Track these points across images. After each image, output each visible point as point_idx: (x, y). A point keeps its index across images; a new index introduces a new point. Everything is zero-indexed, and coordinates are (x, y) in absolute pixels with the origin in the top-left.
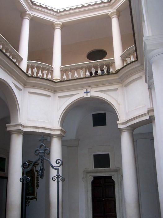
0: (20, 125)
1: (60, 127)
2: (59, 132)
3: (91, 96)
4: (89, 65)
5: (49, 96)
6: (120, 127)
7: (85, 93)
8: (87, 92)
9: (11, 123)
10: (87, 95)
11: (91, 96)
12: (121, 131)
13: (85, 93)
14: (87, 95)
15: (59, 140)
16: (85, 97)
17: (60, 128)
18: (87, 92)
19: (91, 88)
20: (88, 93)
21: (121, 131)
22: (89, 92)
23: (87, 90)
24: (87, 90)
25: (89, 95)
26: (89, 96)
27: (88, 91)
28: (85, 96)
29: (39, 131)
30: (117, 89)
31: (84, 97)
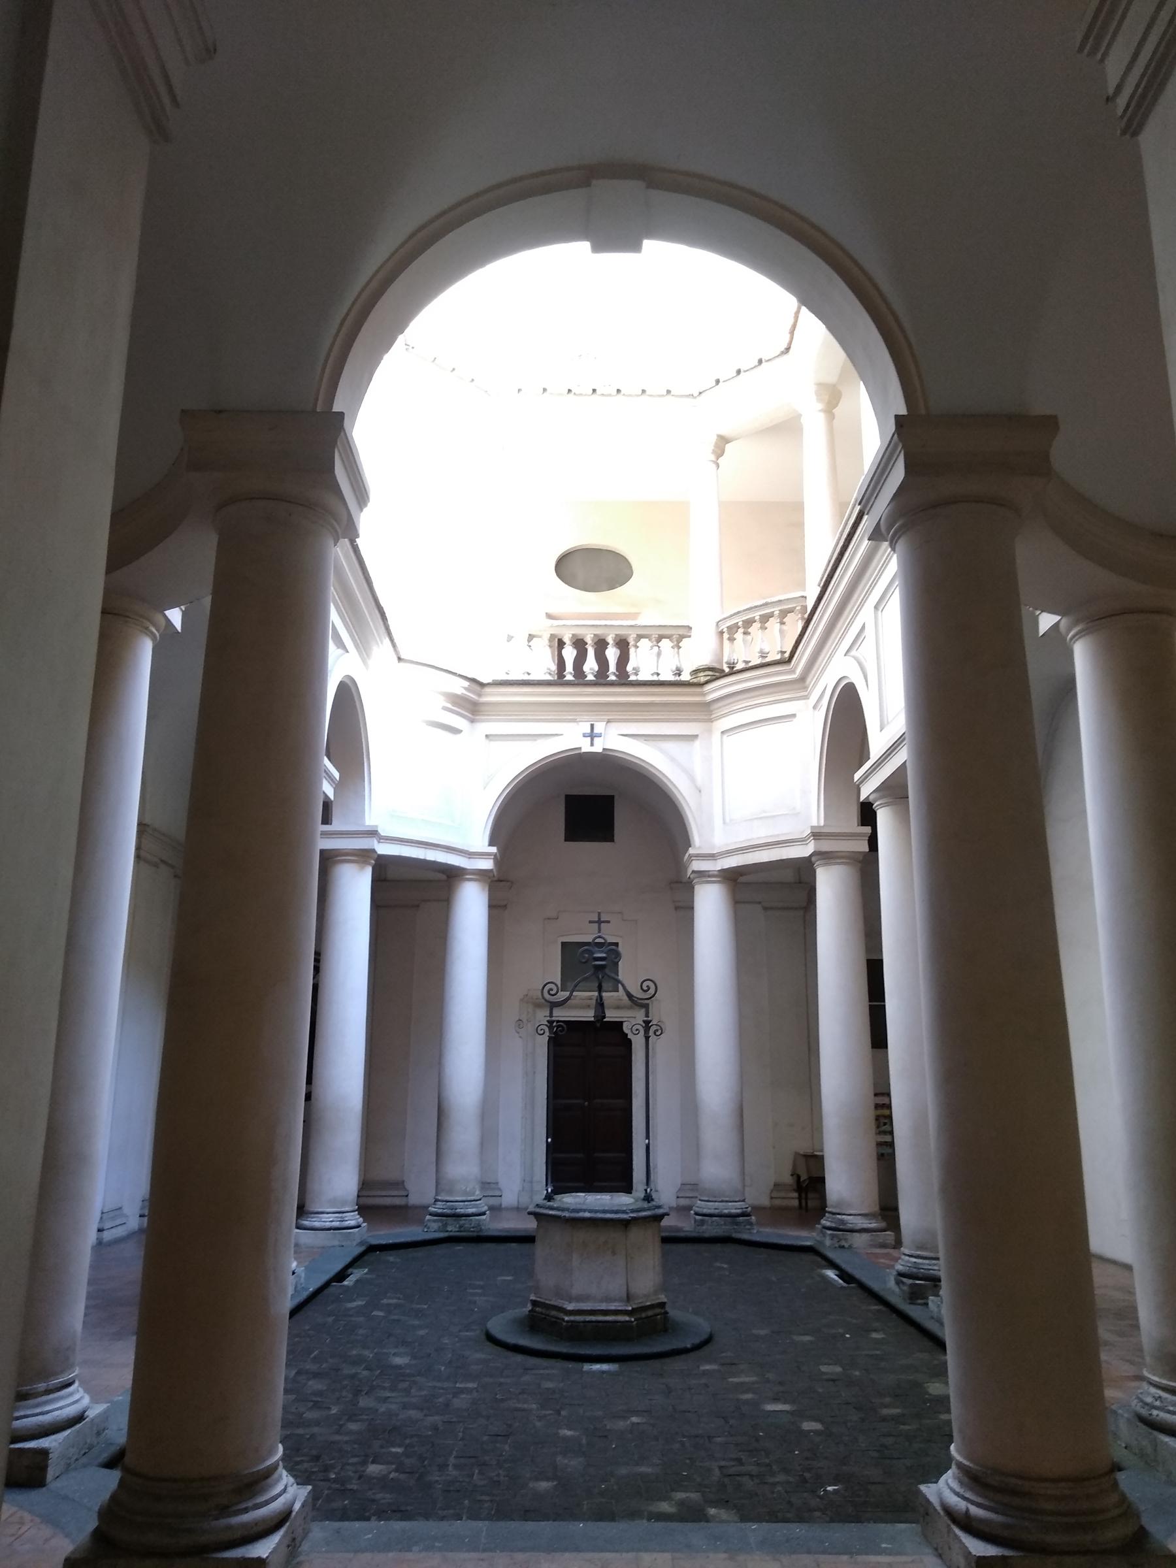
0: (373, 833)
1: (491, 844)
2: (487, 864)
3: (604, 749)
4: (599, 632)
5: (455, 731)
6: (697, 865)
7: (585, 735)
8: (592, 735)
9: (334, 822)
10: (592, 744)
11: (604, 749)
13: (585, 735)
14: (592, 744)
16: (583, 750)
18: (592, 735)
19: (609, 721)
20: (596, 740)
22: (599, 735)
23: (592, 726)
24: (592, 726)
25: (598, 748)
26: (600, 751)
27: (596, 731)
28: (586, 747)
29: (428, 859)
30: (696, 736)
31: (580, 748)
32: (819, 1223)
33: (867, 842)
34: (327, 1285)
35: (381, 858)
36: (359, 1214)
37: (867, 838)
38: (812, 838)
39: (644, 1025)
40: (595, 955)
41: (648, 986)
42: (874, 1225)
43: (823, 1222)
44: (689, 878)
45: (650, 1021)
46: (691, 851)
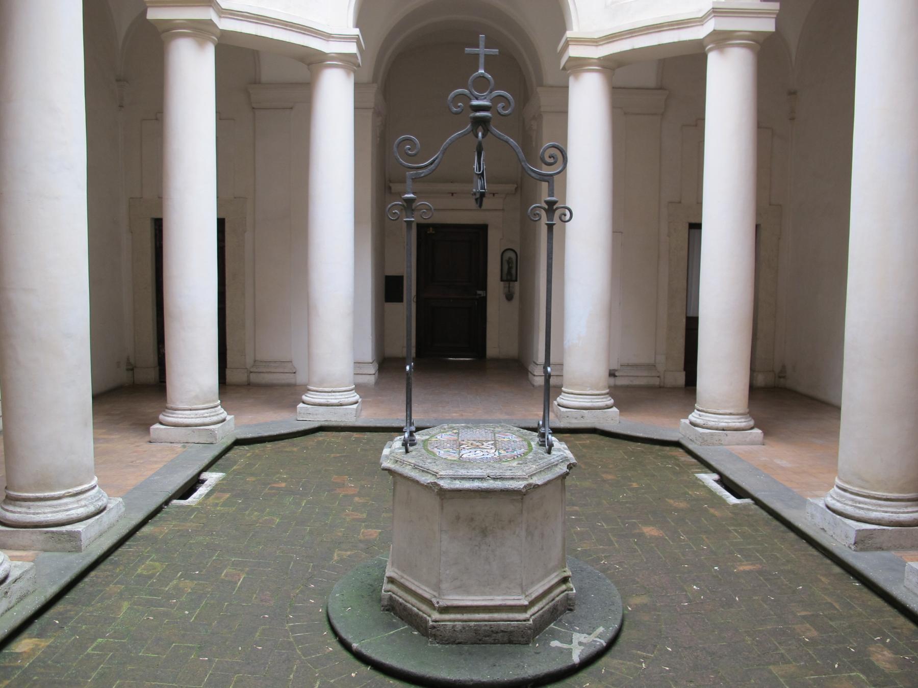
6: (574, 51)
12: (579, 65)
15: (348, 74)
17: (357, 31)
21: (579, 65)
32: (687, 418)
33: (773, 21)
34: (167, 502)
35: (225, 34)
36: (222, 407)
37: (775, 16)
38: (713, 15)
39: (546, 207)
40: (475, 103)
41: (550, 157)
42: (743, 425)
43: (690, 417)
44: (564, 68)
45: (555, 202)
46: (569, 34)
